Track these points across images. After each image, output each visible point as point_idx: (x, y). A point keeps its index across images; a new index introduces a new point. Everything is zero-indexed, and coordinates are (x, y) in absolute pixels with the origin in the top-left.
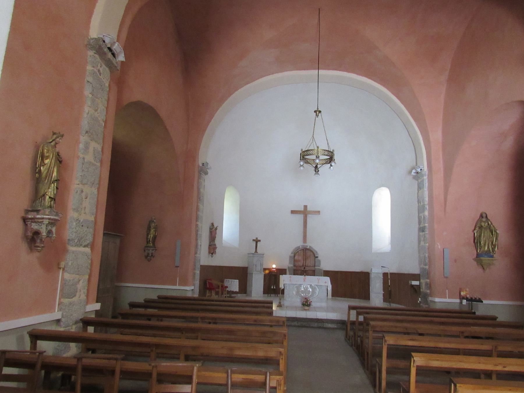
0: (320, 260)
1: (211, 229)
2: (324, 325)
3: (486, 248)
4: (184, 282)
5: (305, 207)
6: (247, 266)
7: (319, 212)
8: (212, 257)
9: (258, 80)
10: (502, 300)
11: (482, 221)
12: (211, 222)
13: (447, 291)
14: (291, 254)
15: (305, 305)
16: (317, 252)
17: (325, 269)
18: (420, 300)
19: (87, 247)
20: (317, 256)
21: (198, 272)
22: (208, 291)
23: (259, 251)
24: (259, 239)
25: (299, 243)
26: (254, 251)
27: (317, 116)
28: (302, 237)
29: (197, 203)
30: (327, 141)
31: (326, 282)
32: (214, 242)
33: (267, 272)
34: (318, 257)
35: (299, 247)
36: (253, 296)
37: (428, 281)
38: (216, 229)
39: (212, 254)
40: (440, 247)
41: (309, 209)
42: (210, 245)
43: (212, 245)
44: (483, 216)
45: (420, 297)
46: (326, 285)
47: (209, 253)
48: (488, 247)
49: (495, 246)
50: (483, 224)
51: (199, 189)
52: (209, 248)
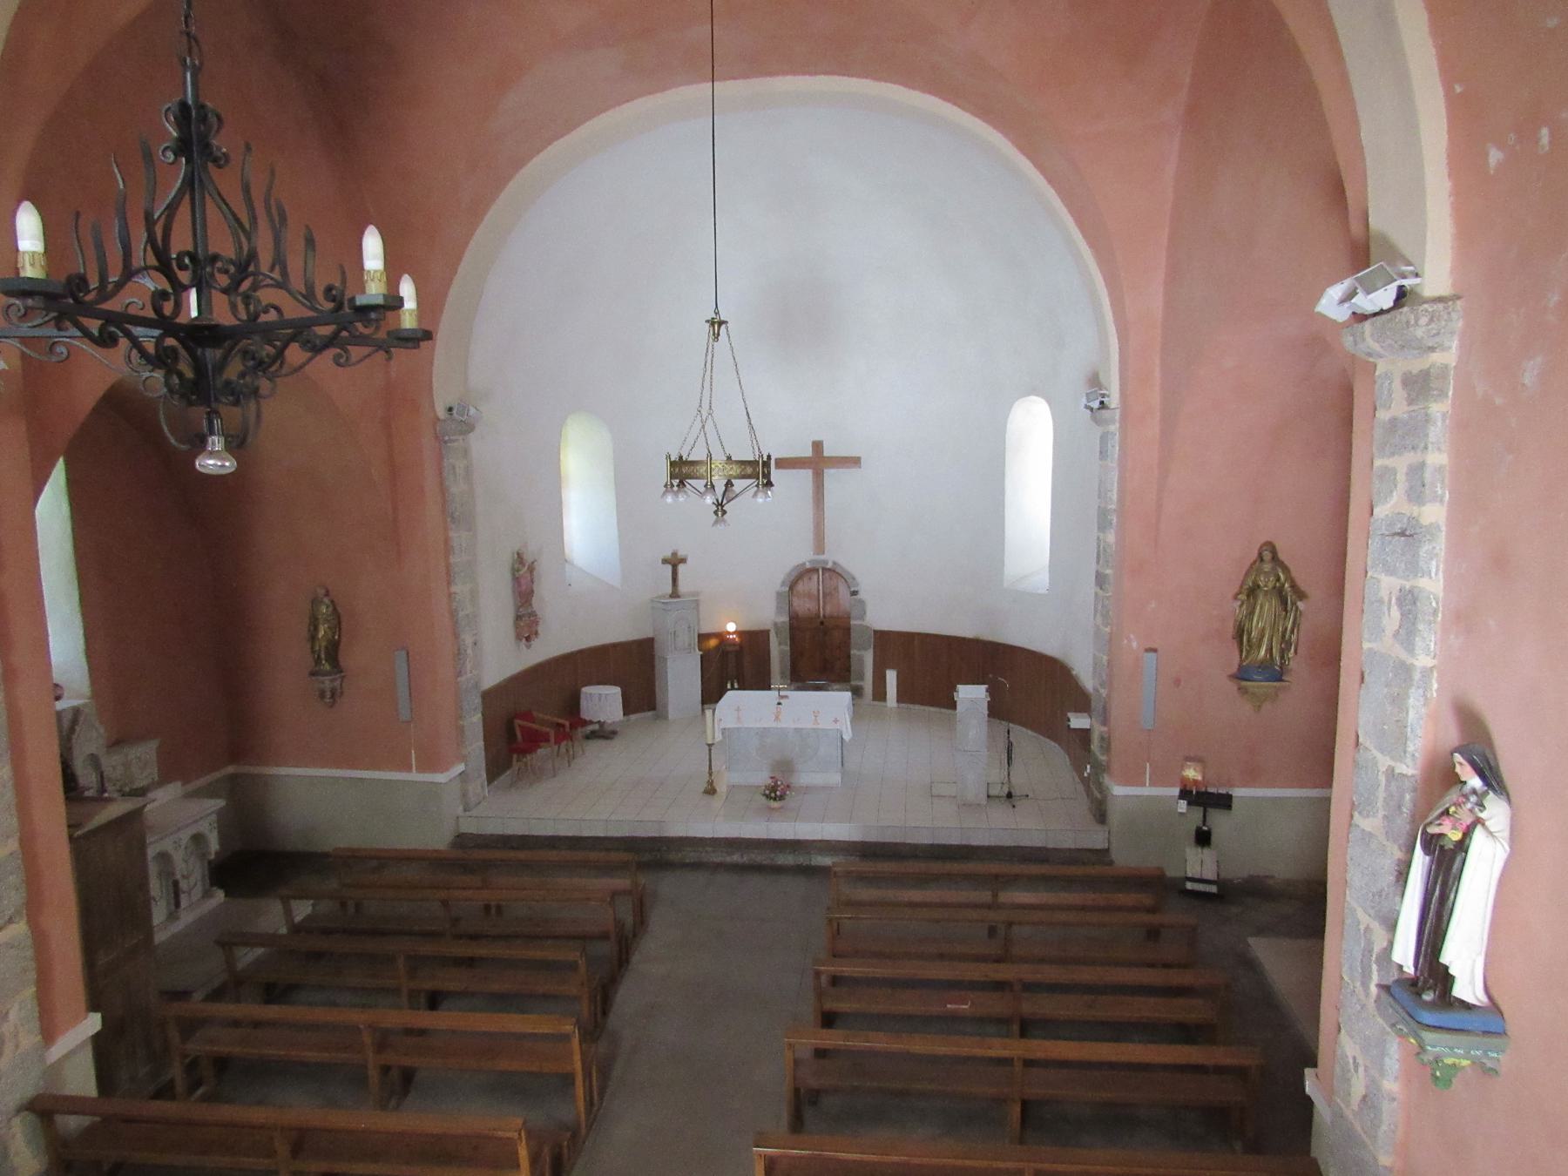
0: (863, 602)
1: (514, 571)
2: (813, 859)
3: (1263, 652)
4: (431, 762)
5: (818, 446)
6: (650, 635)
7: (854, 462)
8: (528, 647)
9: (595, 120)
10: (1302, 787)
11: (1259, 572)
12: (516, 549)
13: (1148, 764)
14: (782, 586)
15: (771, 798)
16: (854, 579)
17: (878, 627)
18: (1088, 771)
19: (13, 922)
20: (856, 589)
21: (476, 719)
22: (515, 756)
23: (683, 587)
24: (681, 554)
25: (804, 555)
26: (669, 590)
27: (717, 336)
28: (810, 536)
29: (446, 529)
30: (747, 413)
31: (836, 721)
32: (531, 605)
33: (713, 643)
34: (857, 592)
35: (804, 564)
36: (670, 717)
37: (1105, 729)
38: (531, 569)
39: (528, 639)
40: (1135, 644)
41: (828, 452)
42: (518, 618)
43: (524, 615)
44: (1264, 558)
45: (1089, 763)
46: (838, 726)
47: (519, 637)
48: (1270, 650)
49: (1289, 644)
50: (1262, 581)
51: (443, 490)
52: (517, 626)
